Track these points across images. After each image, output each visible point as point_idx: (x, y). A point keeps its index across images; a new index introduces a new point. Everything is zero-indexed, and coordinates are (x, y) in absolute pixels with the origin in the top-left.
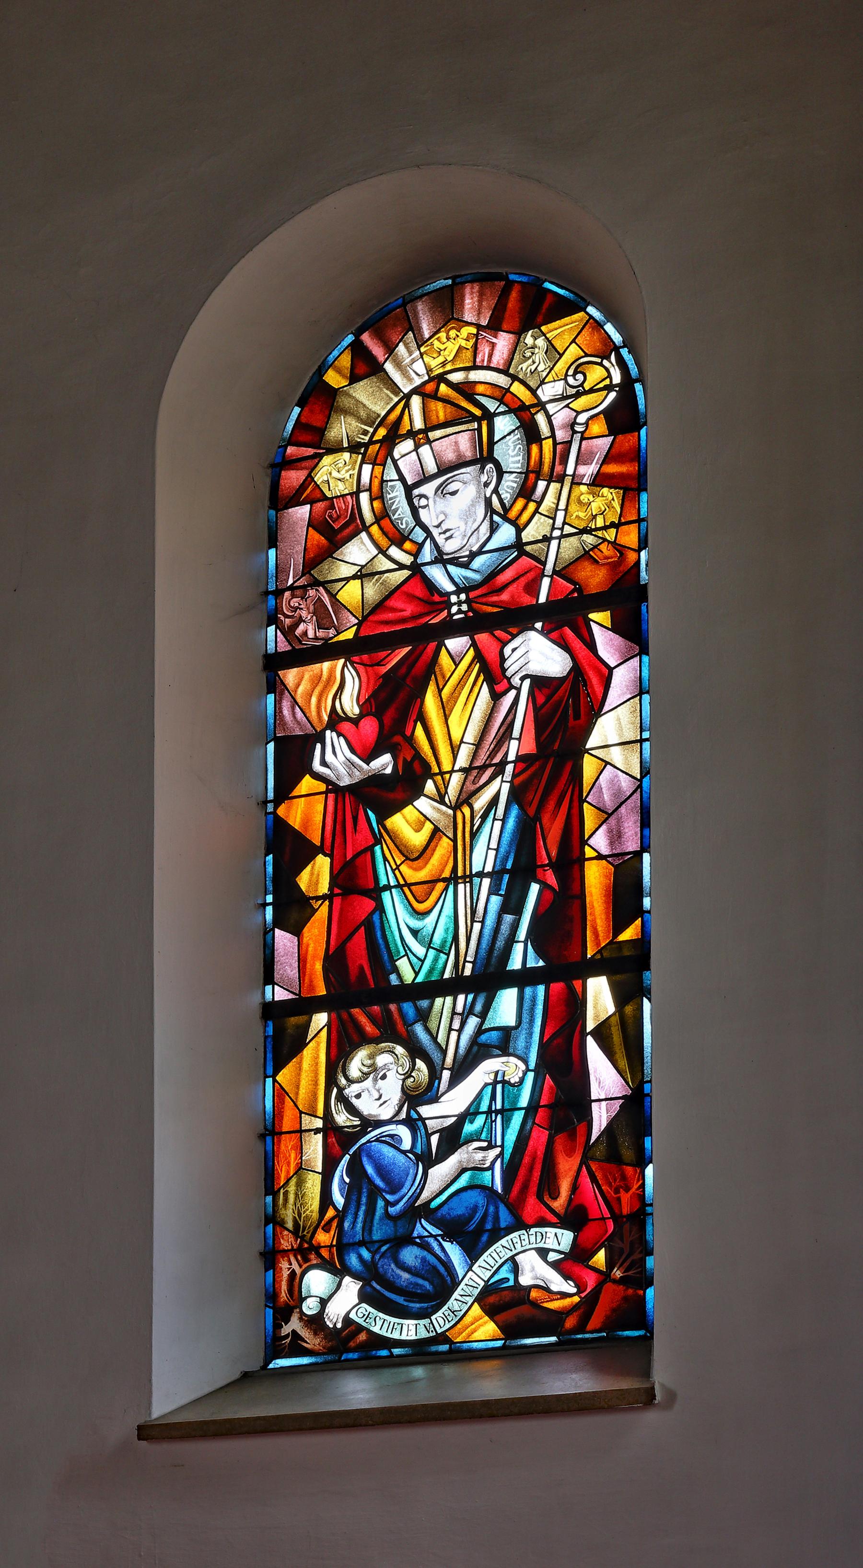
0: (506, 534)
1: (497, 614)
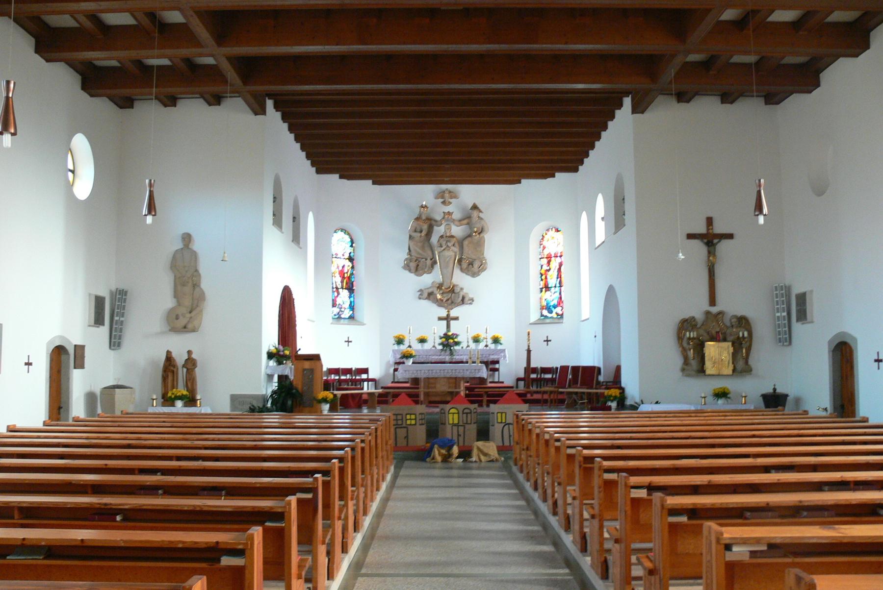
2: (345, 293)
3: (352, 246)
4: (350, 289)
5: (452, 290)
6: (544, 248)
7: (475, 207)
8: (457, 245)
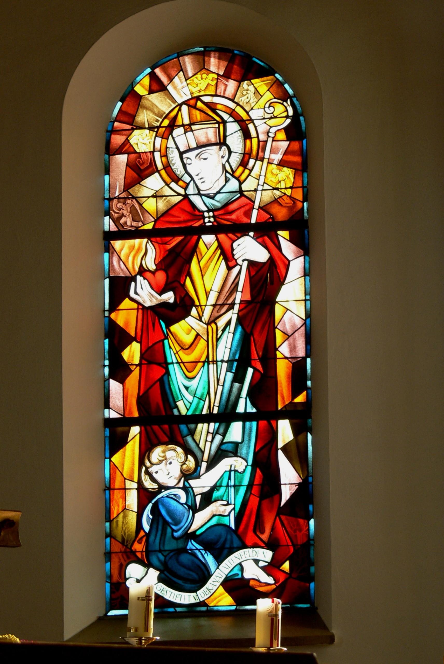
0: (233, 185)
1: (230, 225)
6: (140, 169)
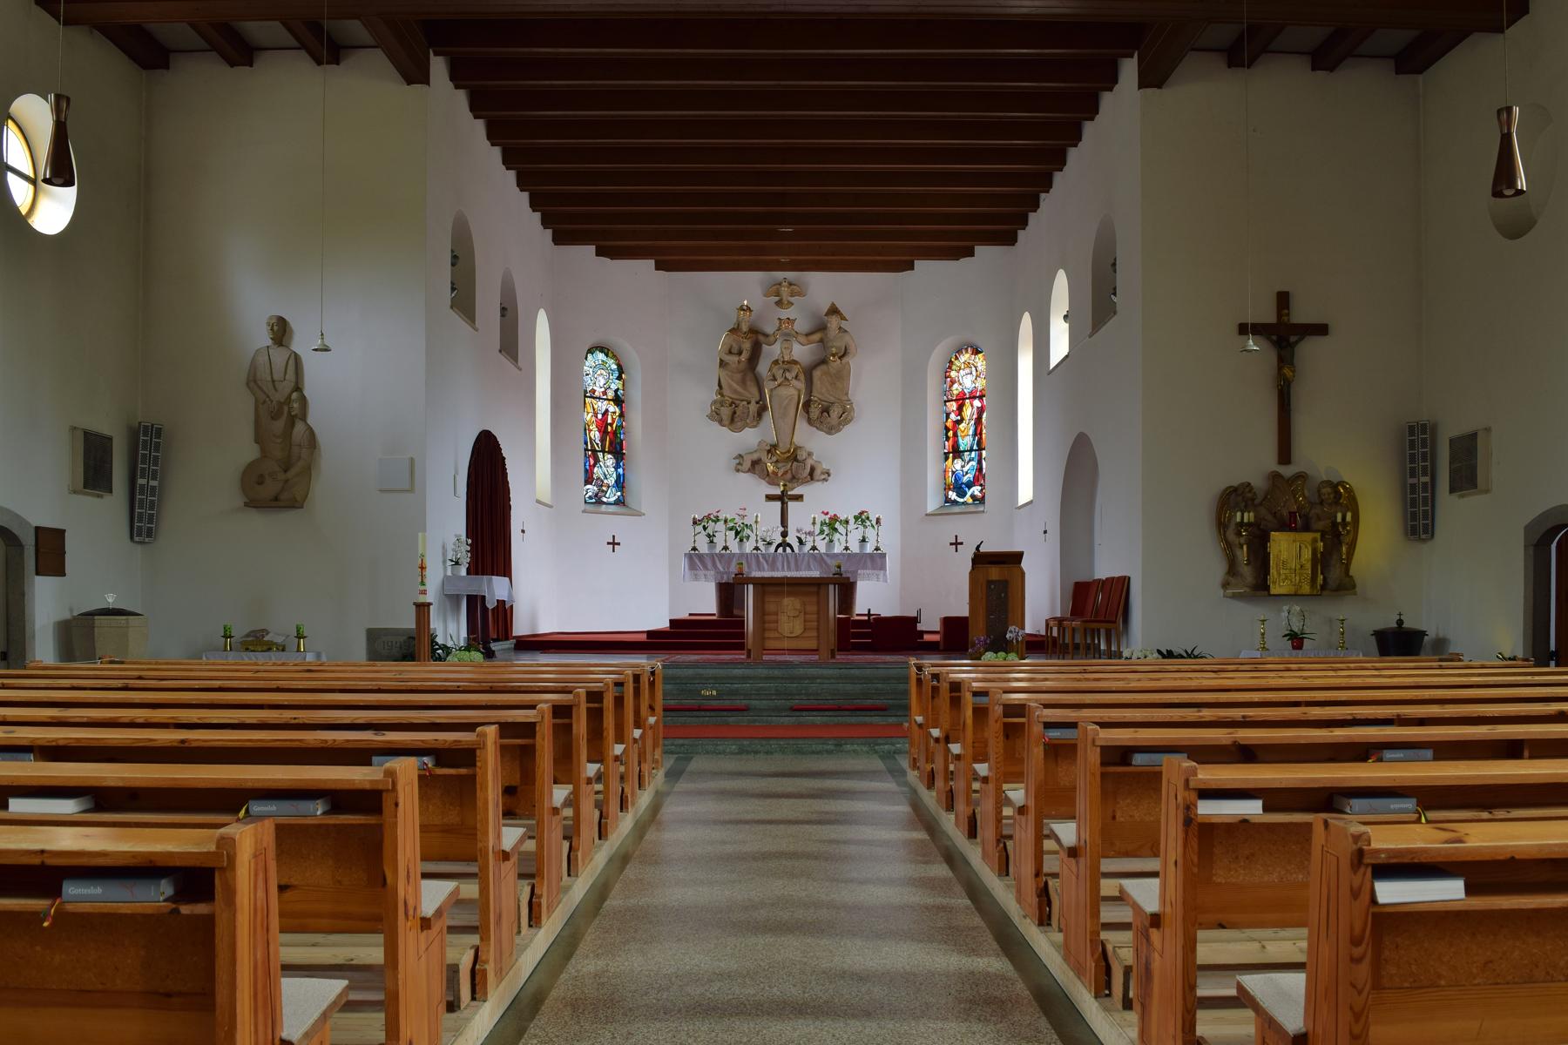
2: (609, 460)
3: (619, 378)
4: (618, 452)
5: (793, 457)
7: (834, 311)
8: (802, 377)
